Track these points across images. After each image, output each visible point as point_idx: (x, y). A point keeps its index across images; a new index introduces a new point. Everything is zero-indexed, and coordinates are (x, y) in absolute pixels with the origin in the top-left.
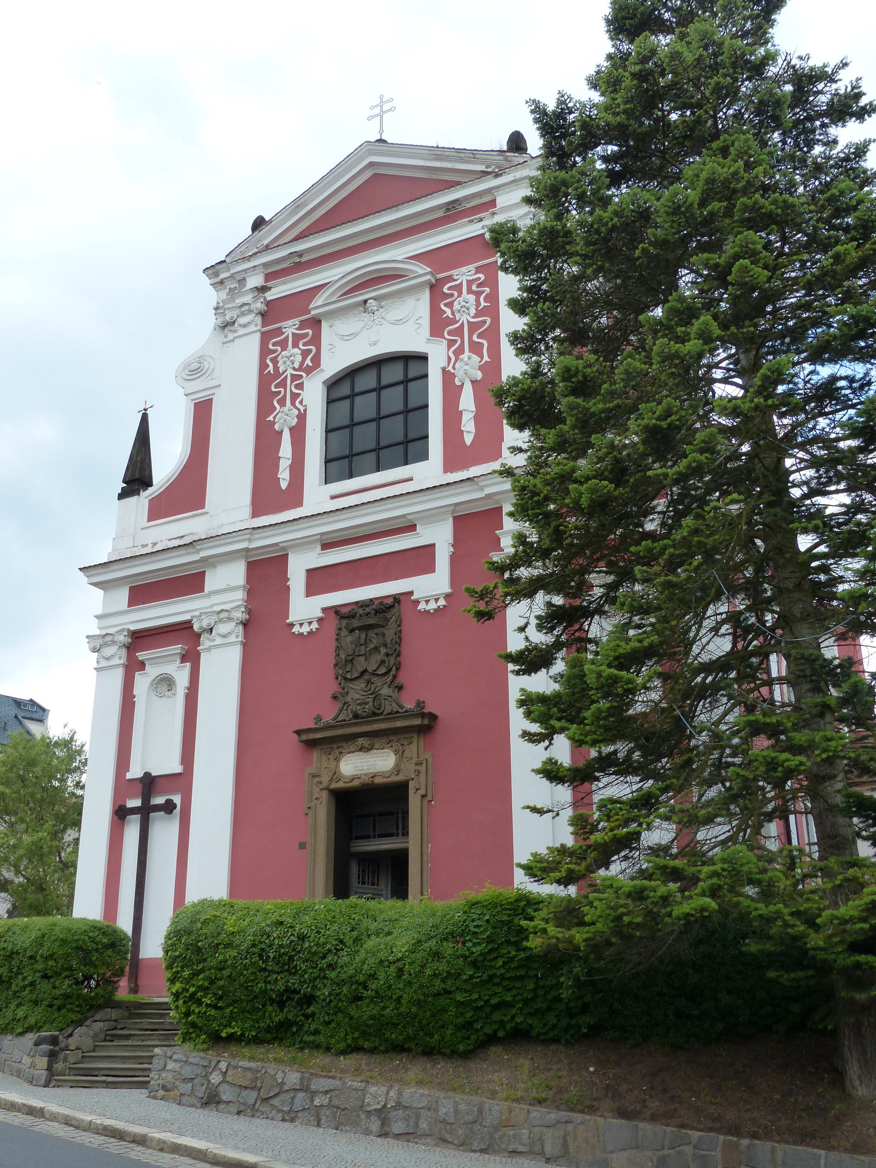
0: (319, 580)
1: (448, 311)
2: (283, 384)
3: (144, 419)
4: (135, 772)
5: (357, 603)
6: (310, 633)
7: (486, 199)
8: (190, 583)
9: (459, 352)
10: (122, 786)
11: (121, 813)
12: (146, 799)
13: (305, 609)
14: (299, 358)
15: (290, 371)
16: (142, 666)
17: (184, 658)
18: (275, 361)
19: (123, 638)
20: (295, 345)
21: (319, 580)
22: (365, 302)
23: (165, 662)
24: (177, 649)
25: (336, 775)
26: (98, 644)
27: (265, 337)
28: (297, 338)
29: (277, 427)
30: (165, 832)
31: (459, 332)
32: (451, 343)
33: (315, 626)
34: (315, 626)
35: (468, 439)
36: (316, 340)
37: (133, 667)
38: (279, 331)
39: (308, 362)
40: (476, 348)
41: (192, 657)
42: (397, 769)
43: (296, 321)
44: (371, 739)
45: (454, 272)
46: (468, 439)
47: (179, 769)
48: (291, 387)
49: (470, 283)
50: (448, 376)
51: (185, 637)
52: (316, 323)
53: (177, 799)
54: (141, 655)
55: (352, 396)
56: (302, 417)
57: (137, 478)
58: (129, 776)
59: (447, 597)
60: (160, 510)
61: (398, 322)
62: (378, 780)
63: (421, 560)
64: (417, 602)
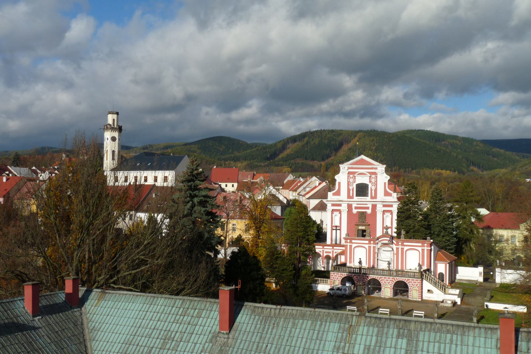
0: (356, 208)
8: (340, 205)
10: (332, 226)
11: (332, 229)
13: (355, 211)
21: (356, 208)
27: (348, 176)
36: (355, 178)
41: (340, 213)
44: (363, 225)
60: (334, 194)
63: (368, 208)
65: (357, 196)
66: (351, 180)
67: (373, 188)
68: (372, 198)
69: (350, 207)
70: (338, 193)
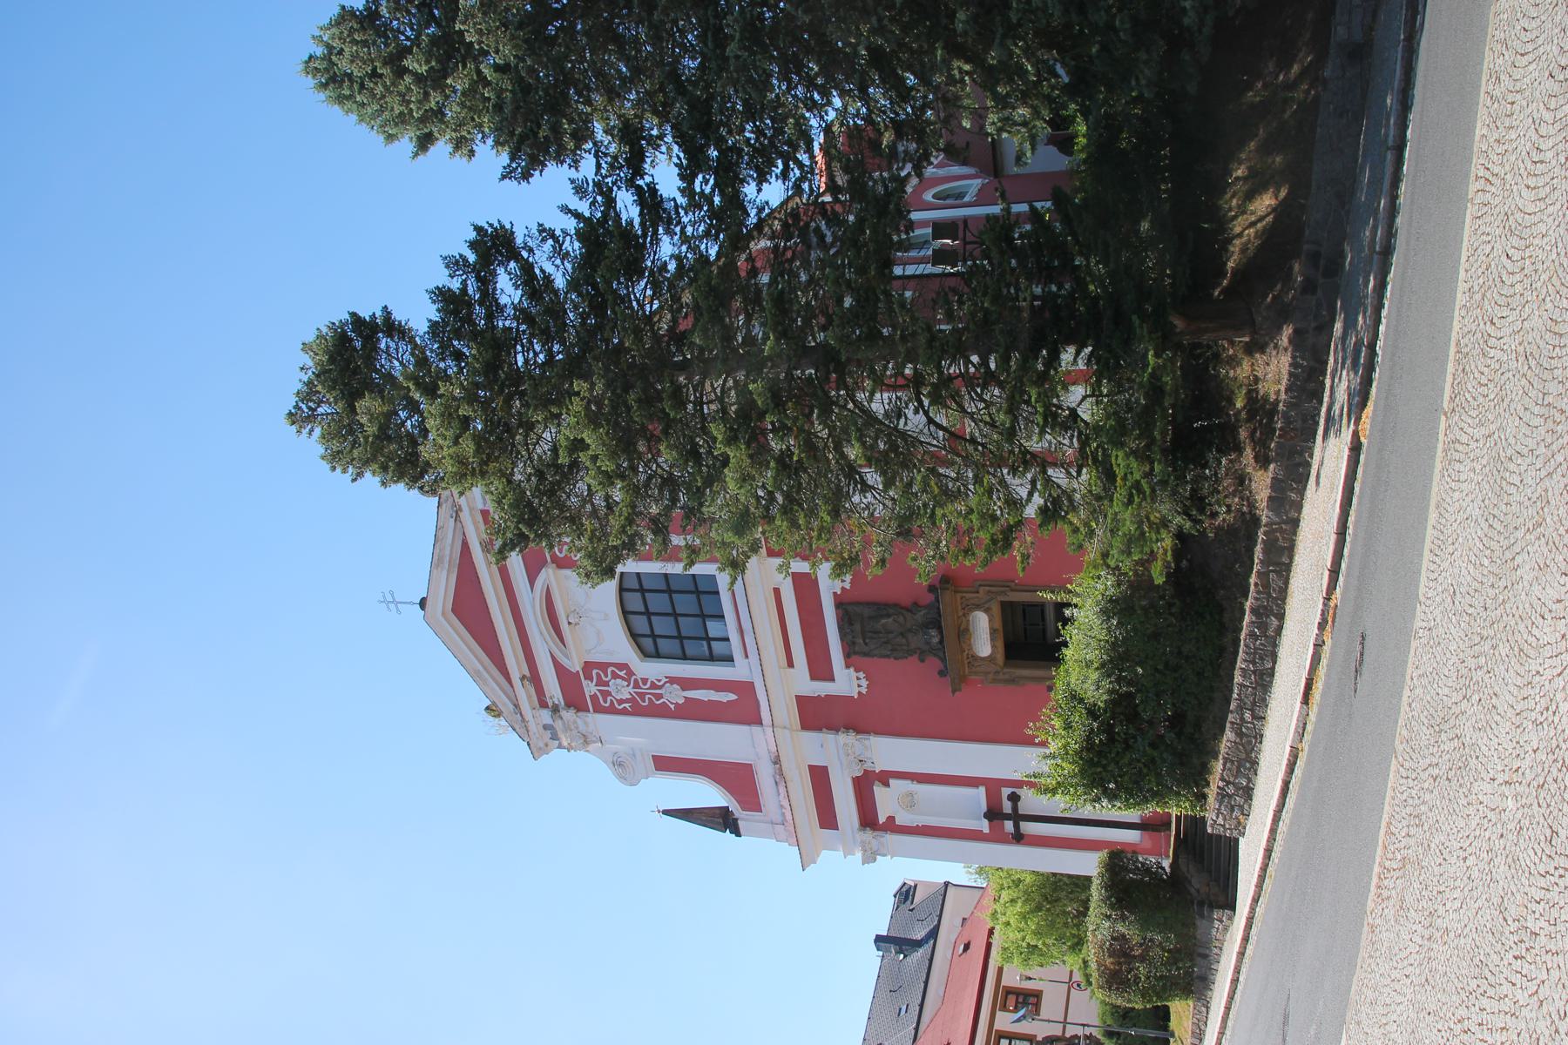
0: (820, 669)
2: (642, 695)
3: (667, 812)
4: (985, 826)
6: (867, 678)
7: (480, 518)
8: (819, 776)
10: (996, 837)
11: (1018, 838)
12: (1008, 817)
13: (846, 682)
15: (630, 689)
16: (891, 819)
17: (887, 785)
18: (621, 702)
20: (607, 684)
23: (887, 801)
24: (878, 790)
25: (991, 659)
26: (869, 857)
27: (599, 709)
28: (600, 683)
29: (681, 701)
30: (1032, 801)
33: (861, 675)
34: (861, 675)
36: (603, 666)
37: (891, 826)
38: (594, 697)
41: (885, 778)
42: (987, 611)
43: (585, 683)
47: (982, 790)
48: (645, 689)
51: (864, 785)
52: (588, 666)
53: (1006, 792)
54: (882, 819)
55: (654, 636)
56: (672, 680)
57: (723, 820)
58: (986, 830)
62: (998, 624)
63: (806, 587)
66: (621, 690)
69: (816, 715)
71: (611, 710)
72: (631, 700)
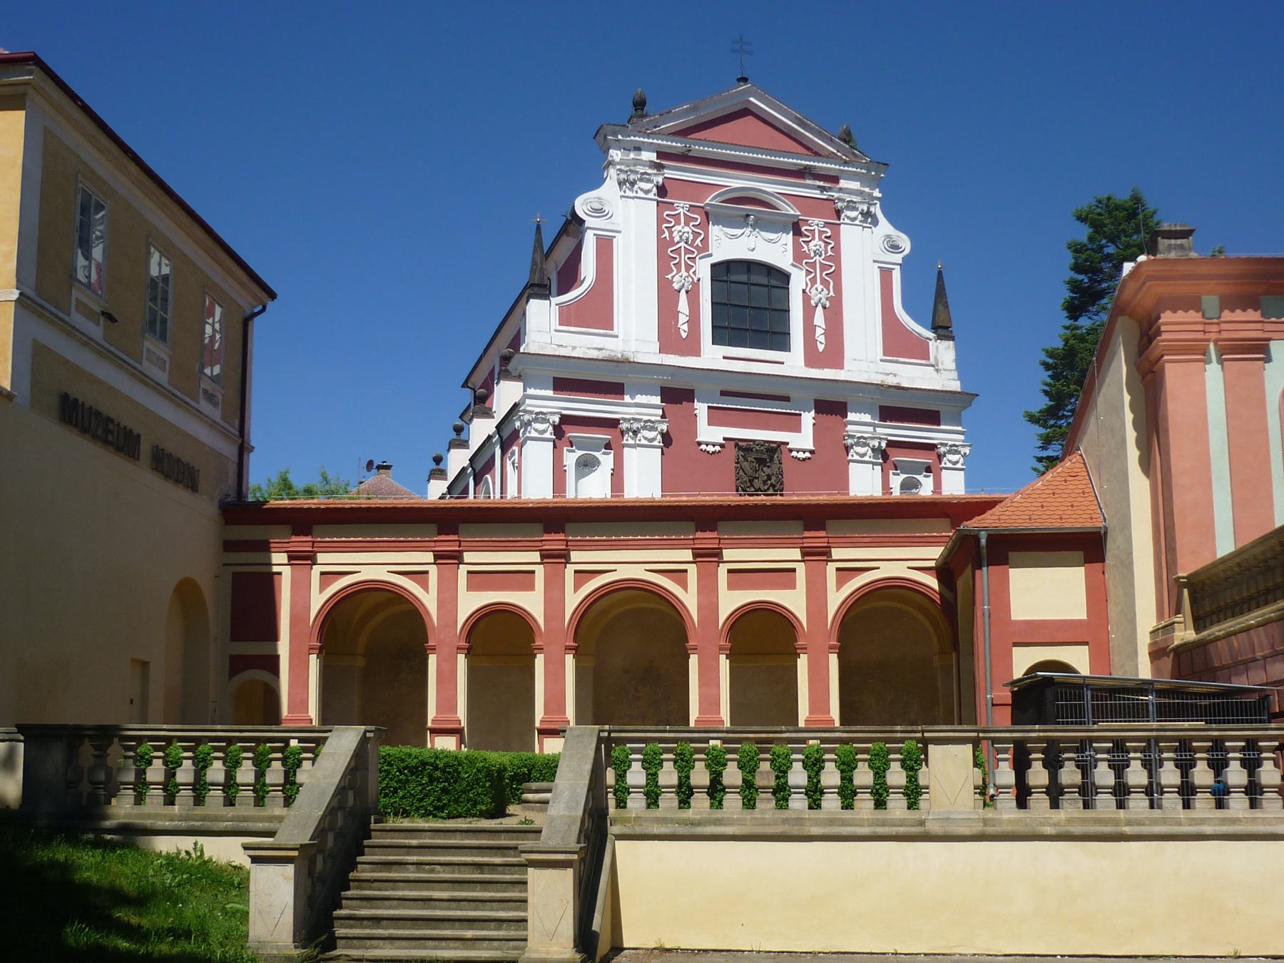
1: (806, 248)
2: (678, 251)
5: (754, 441)
8: (615, 390)
9: (813, 281)
13: (710, 434)
14: (691, 237)
19: (556, 419)
20: (687, 224)
22: (748, 216)
31: (813, 265)
32: (808, 273)
35: (821, 348)
39: (698, 241)
40: (824, 282)
45: (811, 220)
46: (821, 348)
49: (821, 233)
50: (806, 296)
56: (696, 285)
59: (812, 452)
61: (770, 241)
64: (791, 451)
65: (715, 341)
67: (819, 294)
68: (812, 358)
70: (596, 311)
71: (660, 220)
72: (672, 243)
